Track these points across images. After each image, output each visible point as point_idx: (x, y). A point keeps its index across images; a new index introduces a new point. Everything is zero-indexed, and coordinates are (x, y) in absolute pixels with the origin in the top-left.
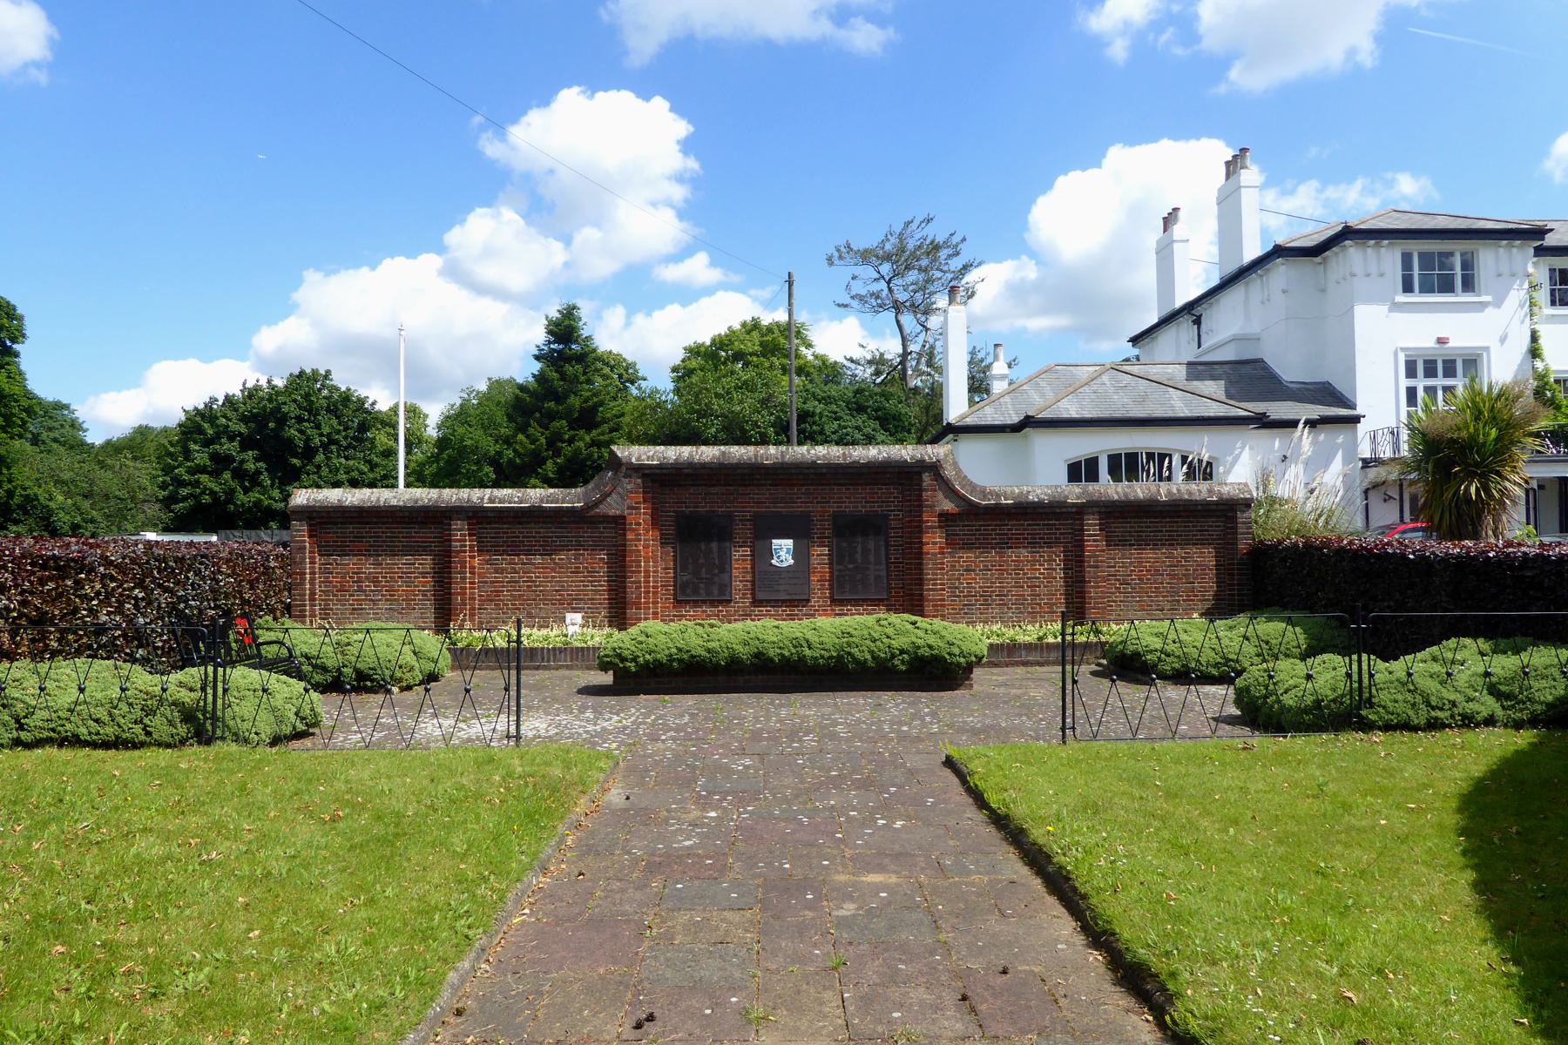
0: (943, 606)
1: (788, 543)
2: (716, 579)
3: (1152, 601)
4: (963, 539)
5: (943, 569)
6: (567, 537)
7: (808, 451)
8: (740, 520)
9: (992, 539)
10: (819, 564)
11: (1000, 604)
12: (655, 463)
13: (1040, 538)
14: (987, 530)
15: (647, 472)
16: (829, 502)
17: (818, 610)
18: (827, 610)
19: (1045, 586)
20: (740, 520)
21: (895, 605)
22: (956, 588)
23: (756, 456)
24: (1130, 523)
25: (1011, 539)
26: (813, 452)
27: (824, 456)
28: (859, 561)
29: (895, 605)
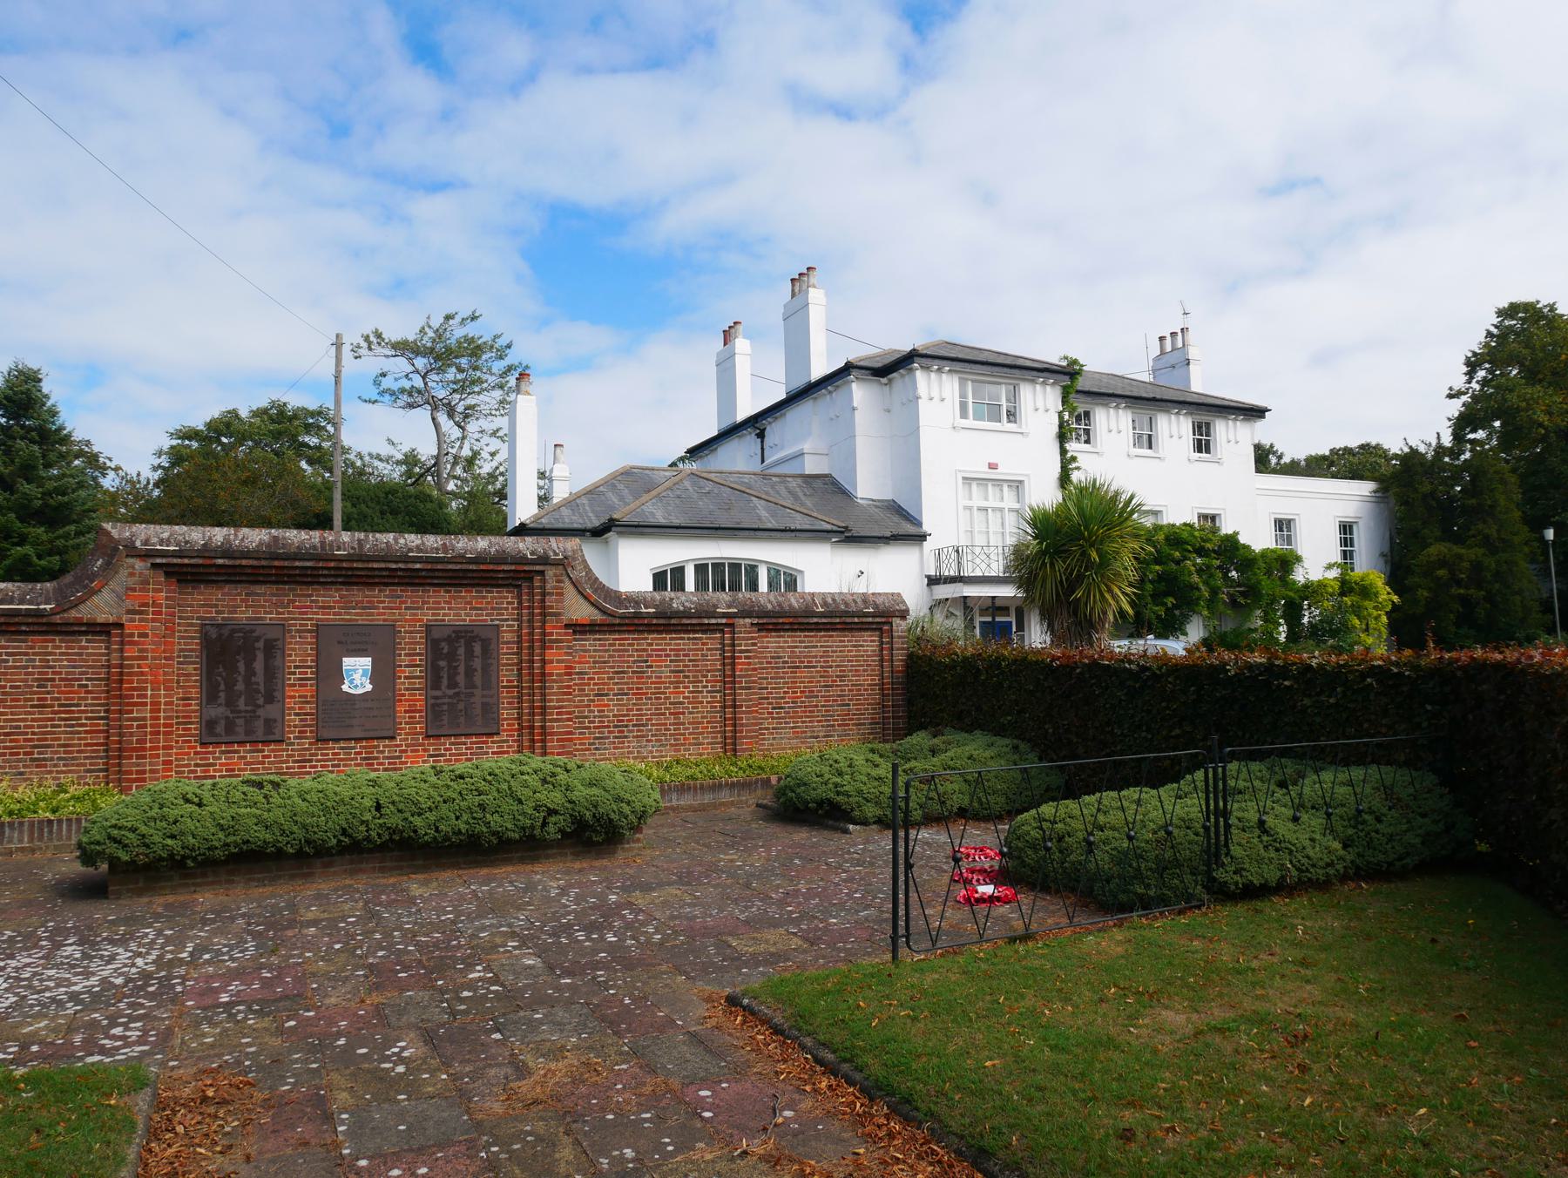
0: (570, 740)
1: (366, 662)
2: (260, 712)
3: (807, 727)
4: (595, 657)
5: (570, 694)
6: (26, 654)
7: (396, 540)
8: (298, 631)
9: (629, 656)
10: (407, 689)
11: (637, 736)
12: (172, 548)
13: (684, 655)
14: (623, 645)
15: (158, 561)
16: (422, 608)
17: (406, 751)
19: (690, 713)
20: (298, 631)
21: (507, 741)
22: (586, 717)
23: (323, 543)
24: (783, 637)
25: (651, 656)
26: (402, 541)
27: (417, 547)
29: (507, 741)
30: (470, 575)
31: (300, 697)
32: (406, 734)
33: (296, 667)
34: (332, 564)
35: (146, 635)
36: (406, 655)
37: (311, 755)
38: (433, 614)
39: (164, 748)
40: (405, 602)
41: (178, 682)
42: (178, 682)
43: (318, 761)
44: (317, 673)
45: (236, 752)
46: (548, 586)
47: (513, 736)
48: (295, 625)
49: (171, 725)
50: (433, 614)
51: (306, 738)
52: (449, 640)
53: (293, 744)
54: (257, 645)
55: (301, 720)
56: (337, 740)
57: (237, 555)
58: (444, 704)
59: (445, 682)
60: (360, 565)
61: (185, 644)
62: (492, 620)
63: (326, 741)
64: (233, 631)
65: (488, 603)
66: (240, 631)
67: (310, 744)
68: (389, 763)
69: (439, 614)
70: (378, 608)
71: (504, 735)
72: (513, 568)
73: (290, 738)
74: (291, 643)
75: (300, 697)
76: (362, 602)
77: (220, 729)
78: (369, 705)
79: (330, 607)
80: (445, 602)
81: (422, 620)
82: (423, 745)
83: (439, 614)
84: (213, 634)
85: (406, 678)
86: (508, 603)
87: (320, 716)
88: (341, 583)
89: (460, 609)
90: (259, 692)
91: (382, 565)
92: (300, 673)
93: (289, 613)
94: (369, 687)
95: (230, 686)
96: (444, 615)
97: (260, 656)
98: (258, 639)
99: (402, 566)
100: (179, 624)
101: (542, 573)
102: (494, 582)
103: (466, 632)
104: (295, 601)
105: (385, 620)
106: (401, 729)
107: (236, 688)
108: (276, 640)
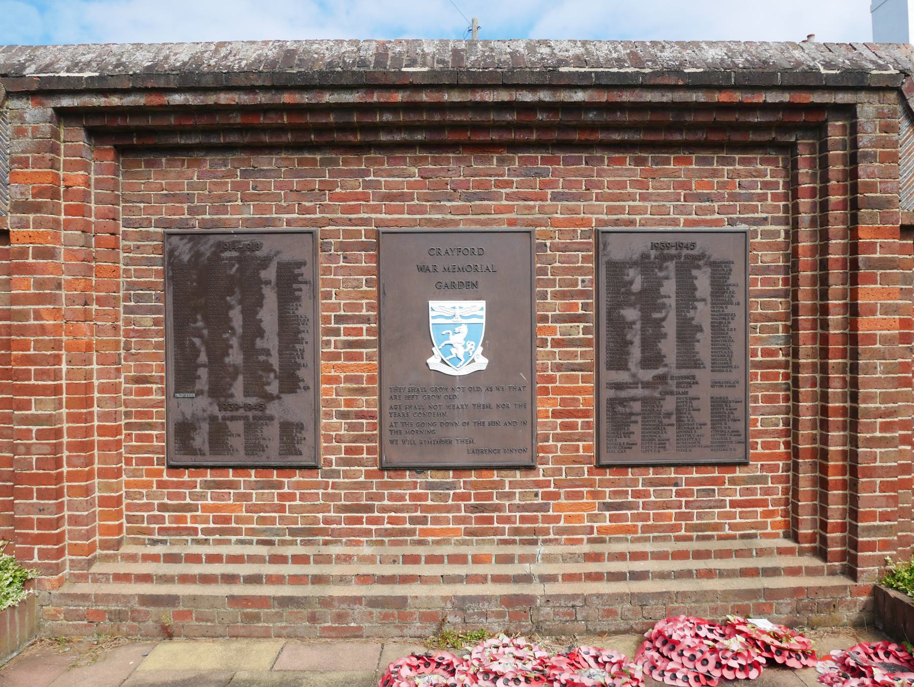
2: (273, 409)
10: (559, 368)
15: (66, 102)
17: (556, 496)
20: (343, 247)
27: (577, 58)
30: (690, 118)
31: (348, 379)
32: (557, 460)
33: (340, 319)
34: (399, 97)
35: (50, 254)
36: (555, 295)
37: (370, 497)
38: (611, 210)
39: (103, 473)
41: (127, 348)
42: (127, 348)
43: (384, 509)
44: (379, 332)
45: (231, 485)
46: (864, 140)
47: (775, 468)
48: (335, 234)
49: (117, 431)
50: (611, 210)
51: (360, 463)
52: (643, 263)
53: (336, 474)
54: (264, 274)
55: (351, 427)
56: (420, 470)
57: (208, 82)
58: (634, 399)
59: (636, 352)
60: (456, 97)
61: (139, 274)
62: (731, 222)
63: (399, 469)
64: (221, 247)
65: (723, 185)
66: (233, 246)
67: (368, 474)
68: (523, 520)
69: (621, 210)
70: (497, 197)
71: (755, 469)
72: (786, 97)
73: (330, 463)
74: (327, 271)
75: (348, 379)
77: (200, 439)
78: (482, 398)
79: (401, 197)
80: (634, 184)
81: (584, 223)
82: (591, 484)
83: (621, 210)
84: (184, 251)
85: (557, 343)
86: (765, 185)
87: (388, 421)
88: (425, 146)
89: (666, 197)
90: (268, 368)
91: (504, 96)
92: (348, 332)
93: (323, 209)
94: (482, 363)
95: (217, 355)
96: (633, 211)
97: (270, 297)
98: (265, 263)
99: (545, 96)
100: (125, 236)
101: (849, 111)
102: (737, 137)
103: (679, 246)
105: (511, 222)
106: (545, 450)
107: (227, 360)
108: (304, 264)
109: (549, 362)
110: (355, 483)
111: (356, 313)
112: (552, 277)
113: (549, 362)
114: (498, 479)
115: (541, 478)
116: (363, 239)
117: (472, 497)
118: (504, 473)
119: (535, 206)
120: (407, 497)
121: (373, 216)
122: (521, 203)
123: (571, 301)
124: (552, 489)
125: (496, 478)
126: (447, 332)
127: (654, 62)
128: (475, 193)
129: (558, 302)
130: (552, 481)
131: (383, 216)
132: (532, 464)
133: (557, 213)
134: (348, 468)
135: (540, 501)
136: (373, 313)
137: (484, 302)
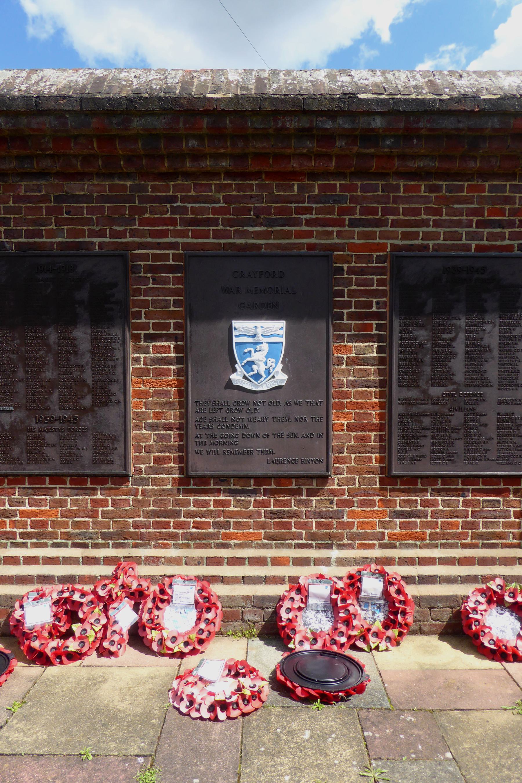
2: (87, 422)
8: (151, 269)
10: (353, 384)
18: (371, 503)
20: (151, 269)
28: (459, 377)
31: (157, 393)
32: (351, 471)
38: (405, 236)
40: (350, 211)
43: (190, 515)
48: (145, 257)
50: (405, 236)
53: (144, 481)
58: (424, 414)
68: (319, 525)
69: (415, 235)
70: (297, 223)
73: (140, 471)
74: (138, 292)
75: (157, 393)
76: (267, 211)
79: (208, 222)
80: (429, 211)
81: (382, 247)
83: (415, 235)
89: (459, 224)
90: (83, 383)
93: (134, 233)
96: (427, 236)
104: (143, 210)
106: (339, 460)
107: (43, 375)
108: (115, 285)
109: (345, 379)
110: (164, 490)
111: (164, 332)
112: (348, 299)
113: (345, 379)
114: (296, 487)
115: (336, 487)
116: (171, 262)
117: (272, 503)
118: (301, 481)
119: (333, 231)
120: (211, 503)
121: (180, 240)
122: (320, 229)
123: (366, 322)
124: (346, 497)
125: (294, 486)
126: (249, 349)
127: (451, 89)
128: (276, 219)
129: (353, 322)
130: (347, 490)
131: (190, 240)
132: (325, 473)
133: (354, 238)
134: (157, 476)
135: (335, 508)
136: (180, 332)
137: (284, 322)
